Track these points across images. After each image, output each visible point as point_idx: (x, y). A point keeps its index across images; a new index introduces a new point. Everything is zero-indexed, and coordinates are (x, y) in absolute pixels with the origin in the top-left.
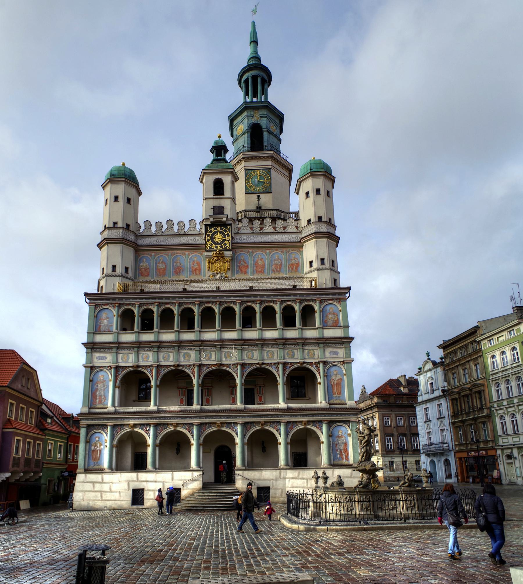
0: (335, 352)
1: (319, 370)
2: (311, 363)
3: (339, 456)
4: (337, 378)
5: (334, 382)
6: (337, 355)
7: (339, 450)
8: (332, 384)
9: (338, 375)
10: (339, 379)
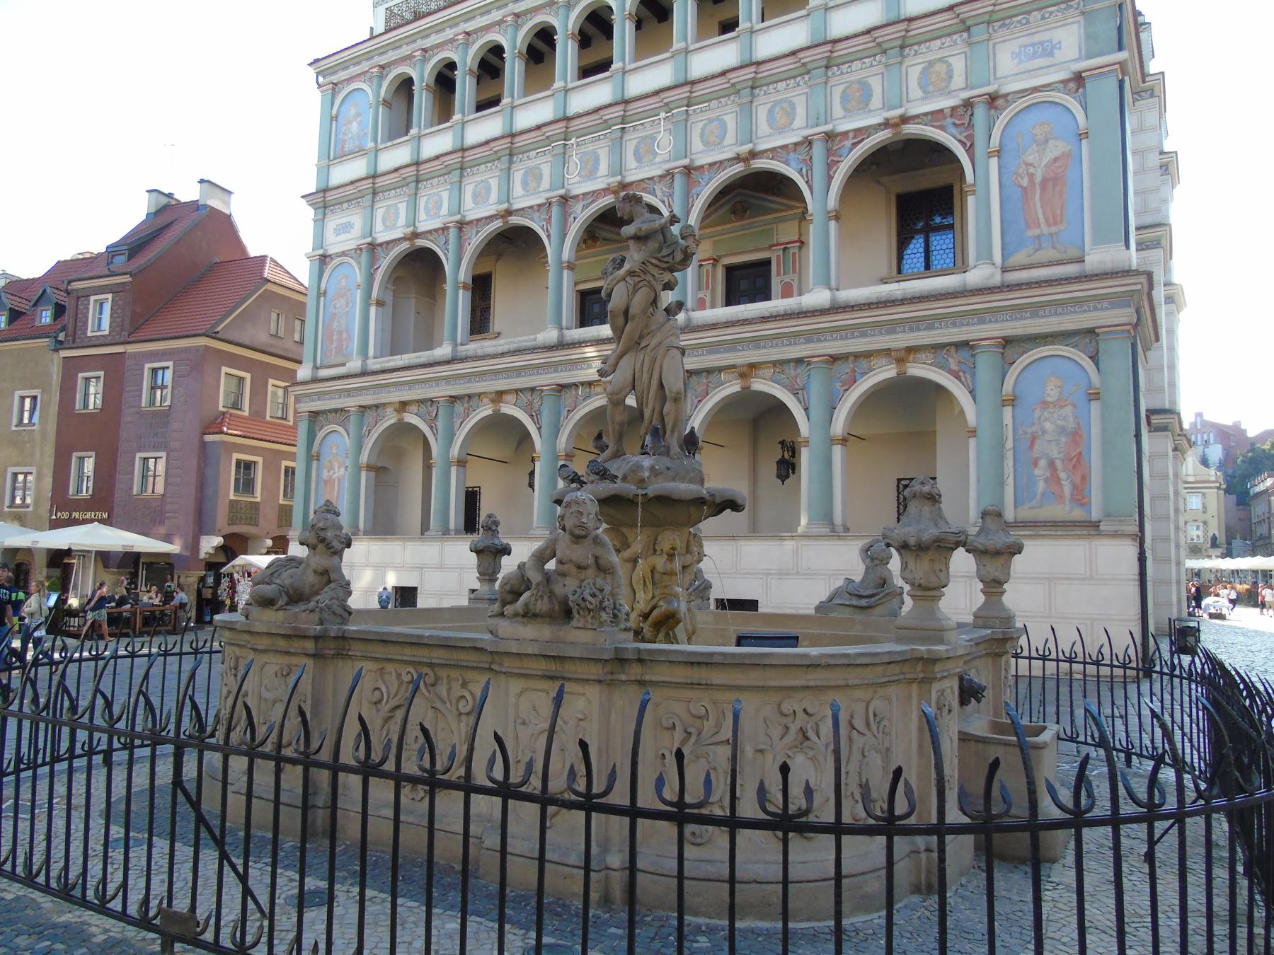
0: (1041, 43)
1: (971, 137)
2: (935, 117)
3: (1041, 486)
4: (1049, 156)
5: (1031, 176)
6: (1051, 54)
7: (1043, 463)
8: (1025, 182)
9: (1051, 143)
10: (1056, 160)
